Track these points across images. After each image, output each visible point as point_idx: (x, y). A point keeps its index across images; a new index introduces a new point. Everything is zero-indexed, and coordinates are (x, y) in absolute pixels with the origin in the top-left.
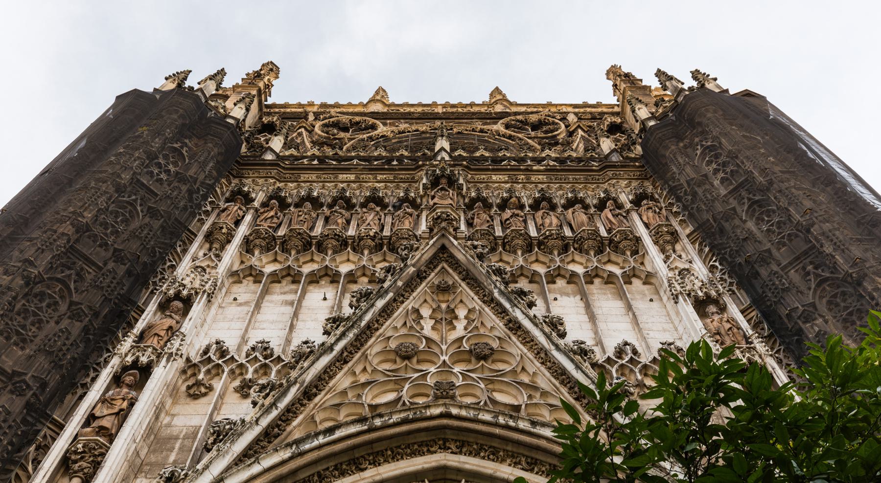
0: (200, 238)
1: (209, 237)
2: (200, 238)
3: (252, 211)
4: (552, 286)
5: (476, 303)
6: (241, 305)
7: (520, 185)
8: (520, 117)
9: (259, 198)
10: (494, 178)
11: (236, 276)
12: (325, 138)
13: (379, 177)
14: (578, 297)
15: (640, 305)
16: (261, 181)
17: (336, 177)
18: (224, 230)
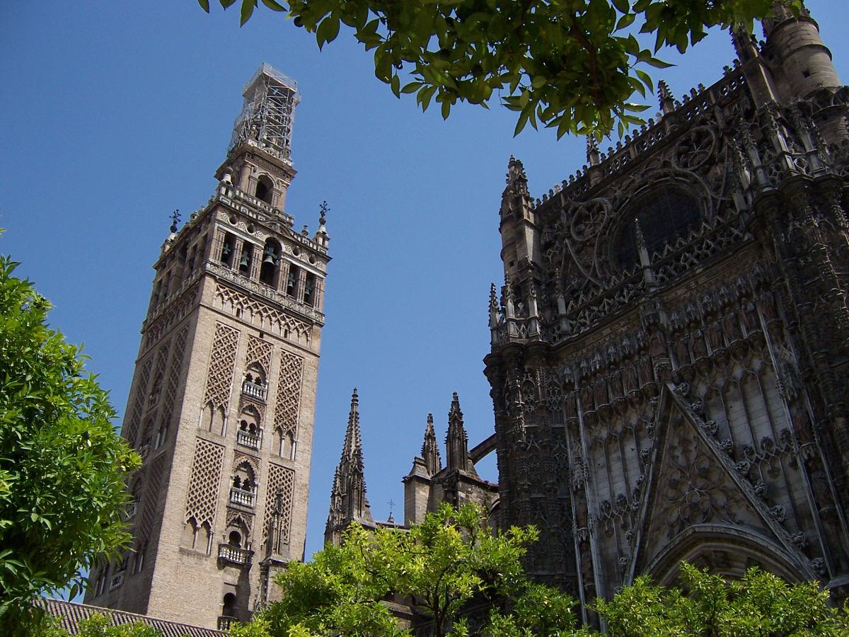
0: (566, 430)
1: (569, 428)
2: (566, 430)
3: (577, 394)
4: (728, 394)
5: (696, 435)
6: (602, 468)
7: (695, 291)
8: (683, 138)
9: (575, 379)
10: (679, 292)
11: (591, 448)
12: (582, 242)
13: (622, 324)
14: (742, 400)
15: (773, 394)
16: (570, 357)
17: (602, 334)
18: (574, 423)
